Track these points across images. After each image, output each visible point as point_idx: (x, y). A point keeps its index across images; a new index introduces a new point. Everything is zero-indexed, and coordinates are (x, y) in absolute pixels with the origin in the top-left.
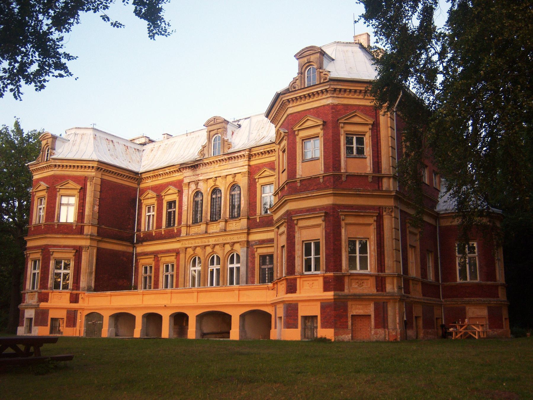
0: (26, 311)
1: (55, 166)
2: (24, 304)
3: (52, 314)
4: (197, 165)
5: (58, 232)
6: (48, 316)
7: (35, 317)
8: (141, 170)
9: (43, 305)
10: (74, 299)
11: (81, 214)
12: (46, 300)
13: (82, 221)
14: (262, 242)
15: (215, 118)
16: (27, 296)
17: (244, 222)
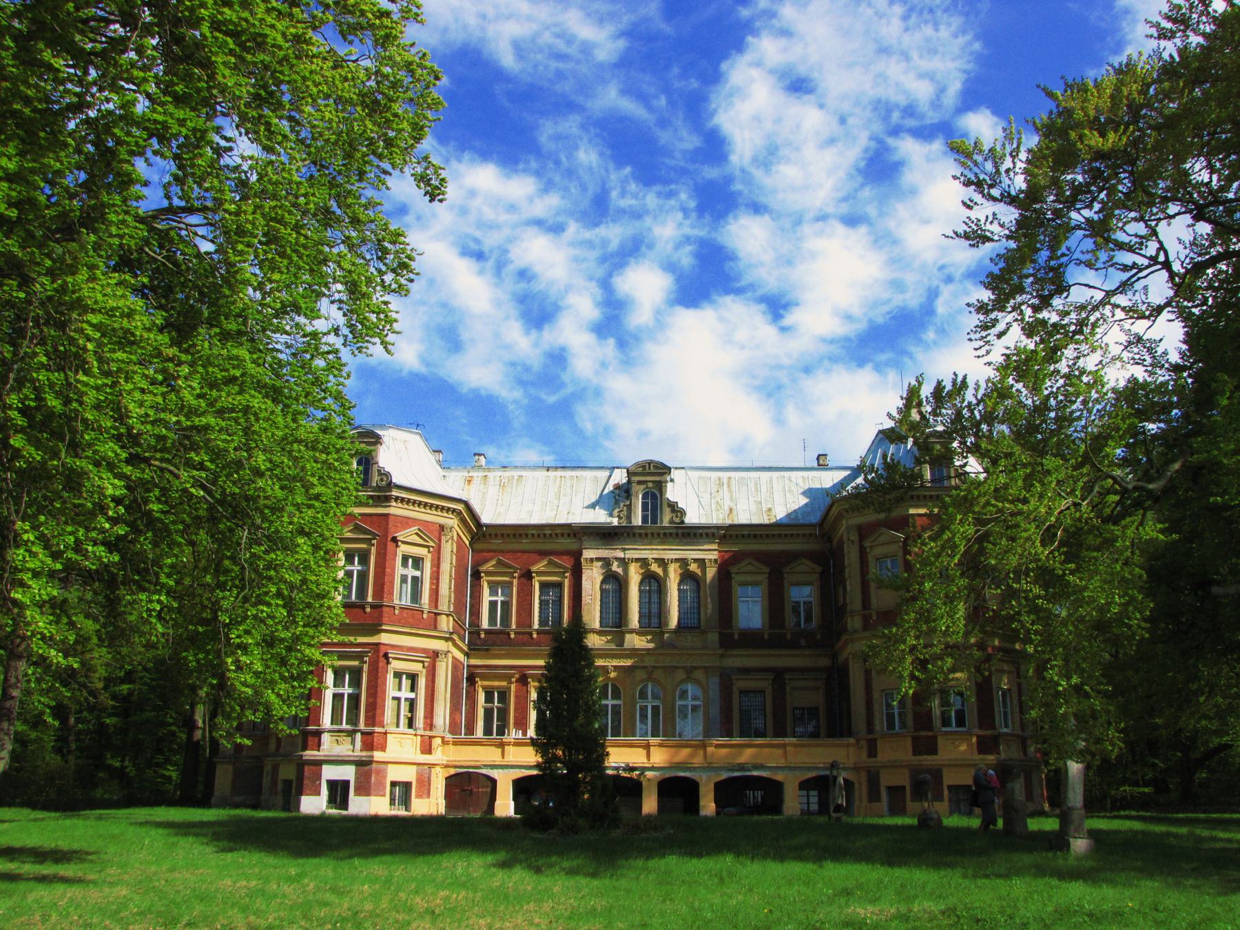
0: (325, 768)
1: (397, 499)
2: (316, 753)
3: (396, 773)
4: (616, 534)
5: (400, 621)
6: (385, 777)
7: (357, 778)
8: (486, 519)
9: (378, 755)
10: (427, 749)
11: (435, 594)
12: (383, 748)
13: (436, 607)
14: (746, 671)
15: (650, 463)
16: (326, 738)
17: (713, 637)
